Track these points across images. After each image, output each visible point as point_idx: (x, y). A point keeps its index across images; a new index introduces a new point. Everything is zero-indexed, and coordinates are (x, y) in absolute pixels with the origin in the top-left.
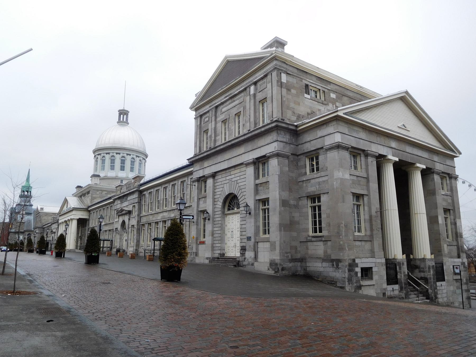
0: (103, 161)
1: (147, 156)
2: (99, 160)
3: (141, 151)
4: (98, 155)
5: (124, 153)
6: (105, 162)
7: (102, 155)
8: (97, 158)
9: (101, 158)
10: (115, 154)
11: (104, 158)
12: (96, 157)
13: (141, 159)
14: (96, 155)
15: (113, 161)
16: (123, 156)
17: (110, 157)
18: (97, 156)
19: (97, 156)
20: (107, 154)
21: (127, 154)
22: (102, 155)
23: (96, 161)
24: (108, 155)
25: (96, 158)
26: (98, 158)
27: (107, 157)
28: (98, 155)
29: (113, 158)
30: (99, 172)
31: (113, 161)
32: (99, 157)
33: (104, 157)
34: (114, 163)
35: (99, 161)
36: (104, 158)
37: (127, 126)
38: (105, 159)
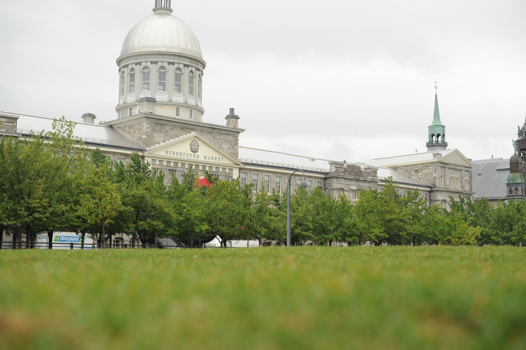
0: (132, 76)
1: (204, 66)
2: (125, 75)
3: (197, 58)
4: (124, 67)
5: (147, 62)
6: (134, 79)
7: (130, 66)
8: (123, 72)
9: (129, 72)
10: (166, 64)
11: (133, 72)
12: (121, 71)
13: (194, 69)
14: (121, 68)
15: (162, 76)
16: (160, 67)
17: (158, 69)
18: (122, 68)
19: (122, 69)
20: (136, 64)
21: (169, 63)
22: (130, 66)
23: (122, 78)
24: (138, 66)
25: (122, 72)
26: (125, 72)
27: (138, 68)
28: (124, 67)
29: (146, 71)
30: (127, 96)
31: (162, 76)
32: (126, 70)
33: (133, 69)
34: (164, 79)
35: (127, 77)
36: (133, 72)
37: (170, 15)
38: (134, 74)
